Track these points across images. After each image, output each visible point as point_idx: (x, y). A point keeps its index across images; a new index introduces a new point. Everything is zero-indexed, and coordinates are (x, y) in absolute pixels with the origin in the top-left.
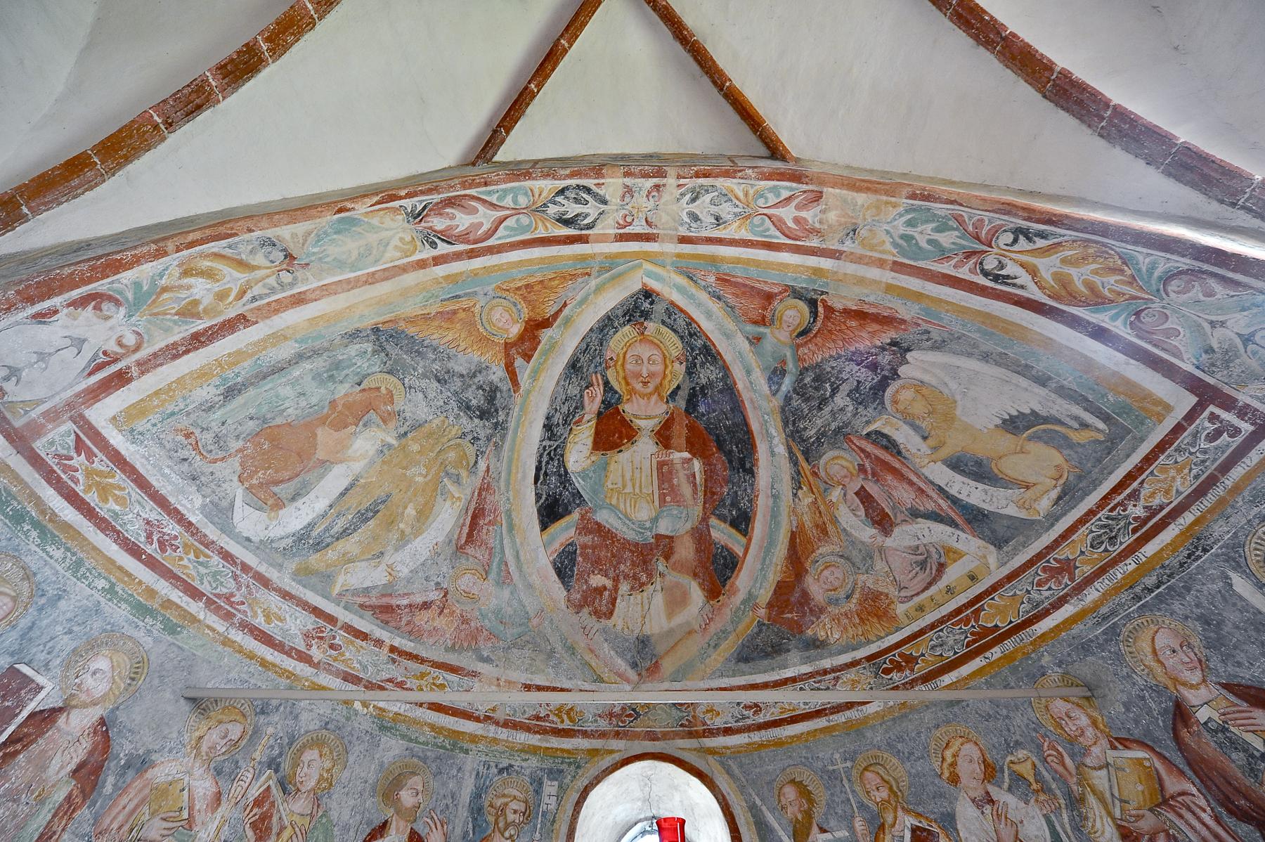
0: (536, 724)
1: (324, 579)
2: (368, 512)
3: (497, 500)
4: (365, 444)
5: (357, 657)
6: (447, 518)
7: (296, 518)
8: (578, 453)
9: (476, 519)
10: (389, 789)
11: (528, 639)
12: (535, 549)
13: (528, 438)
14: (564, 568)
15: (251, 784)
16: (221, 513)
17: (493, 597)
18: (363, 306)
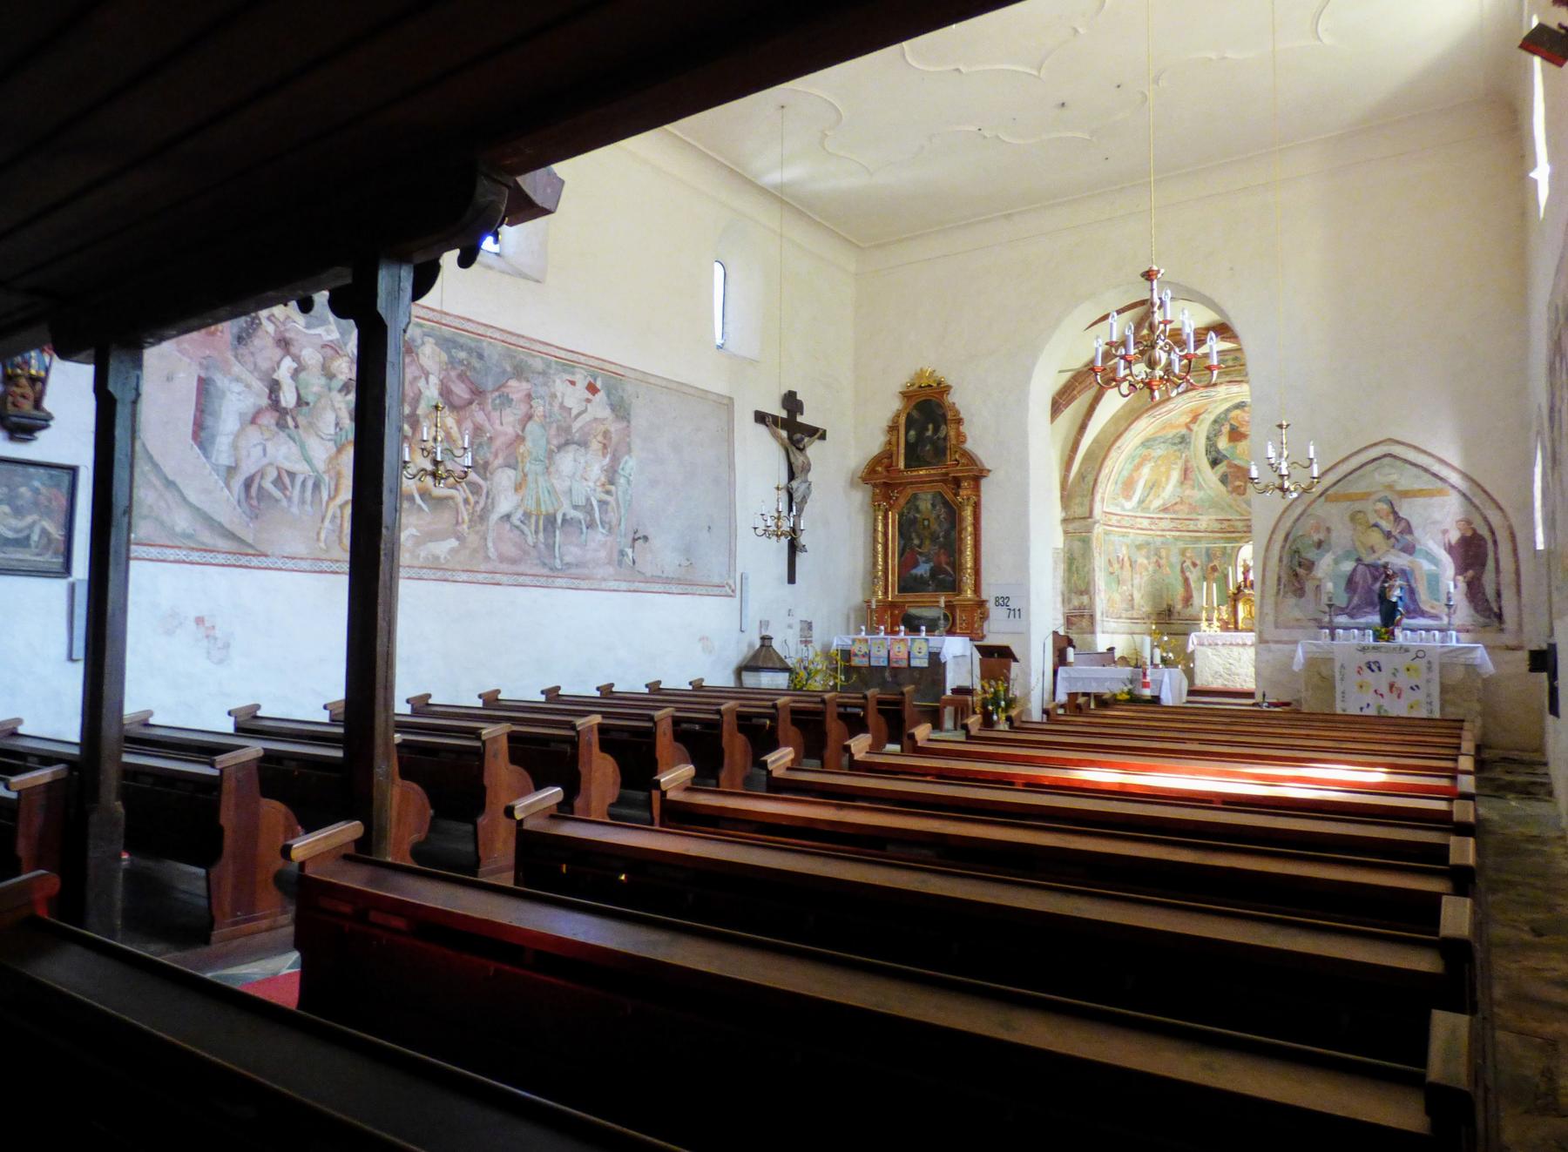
0: (1222, 531)
1: (1146, 509)
2: (1153, 486)
3: (1193, 463)
4: (1146, 471)
5: (1163, 524)
6: (1176, 475)
7: (1136, 498)
8: (1223, 444)
9: (1186, 472)
10: (1183, 552)
11: (1214, 504)
12: (1211, 477)
13: (1200, 442)
14: (1224, 480)
15: (1154, 559)
16: (1123, 508)
17: (1198, 495)
18: (1138, 441)
